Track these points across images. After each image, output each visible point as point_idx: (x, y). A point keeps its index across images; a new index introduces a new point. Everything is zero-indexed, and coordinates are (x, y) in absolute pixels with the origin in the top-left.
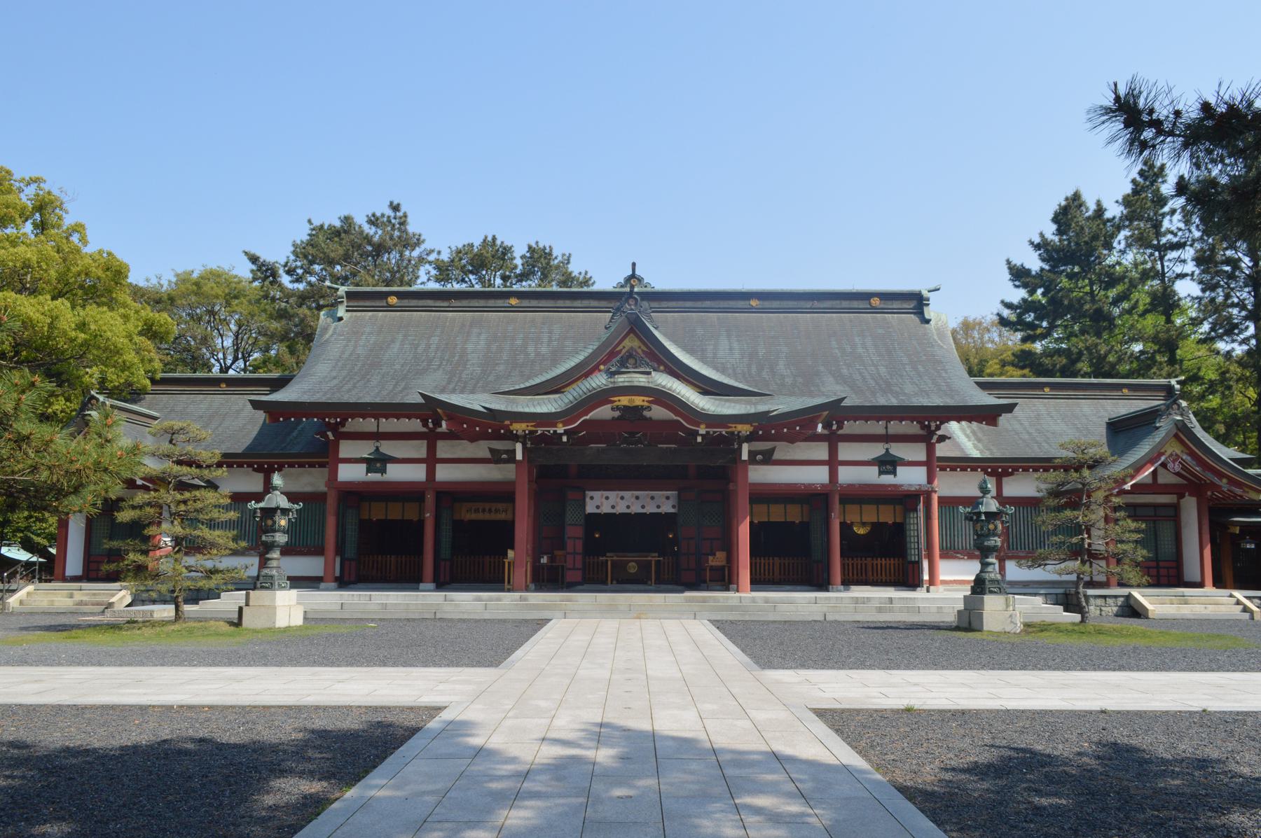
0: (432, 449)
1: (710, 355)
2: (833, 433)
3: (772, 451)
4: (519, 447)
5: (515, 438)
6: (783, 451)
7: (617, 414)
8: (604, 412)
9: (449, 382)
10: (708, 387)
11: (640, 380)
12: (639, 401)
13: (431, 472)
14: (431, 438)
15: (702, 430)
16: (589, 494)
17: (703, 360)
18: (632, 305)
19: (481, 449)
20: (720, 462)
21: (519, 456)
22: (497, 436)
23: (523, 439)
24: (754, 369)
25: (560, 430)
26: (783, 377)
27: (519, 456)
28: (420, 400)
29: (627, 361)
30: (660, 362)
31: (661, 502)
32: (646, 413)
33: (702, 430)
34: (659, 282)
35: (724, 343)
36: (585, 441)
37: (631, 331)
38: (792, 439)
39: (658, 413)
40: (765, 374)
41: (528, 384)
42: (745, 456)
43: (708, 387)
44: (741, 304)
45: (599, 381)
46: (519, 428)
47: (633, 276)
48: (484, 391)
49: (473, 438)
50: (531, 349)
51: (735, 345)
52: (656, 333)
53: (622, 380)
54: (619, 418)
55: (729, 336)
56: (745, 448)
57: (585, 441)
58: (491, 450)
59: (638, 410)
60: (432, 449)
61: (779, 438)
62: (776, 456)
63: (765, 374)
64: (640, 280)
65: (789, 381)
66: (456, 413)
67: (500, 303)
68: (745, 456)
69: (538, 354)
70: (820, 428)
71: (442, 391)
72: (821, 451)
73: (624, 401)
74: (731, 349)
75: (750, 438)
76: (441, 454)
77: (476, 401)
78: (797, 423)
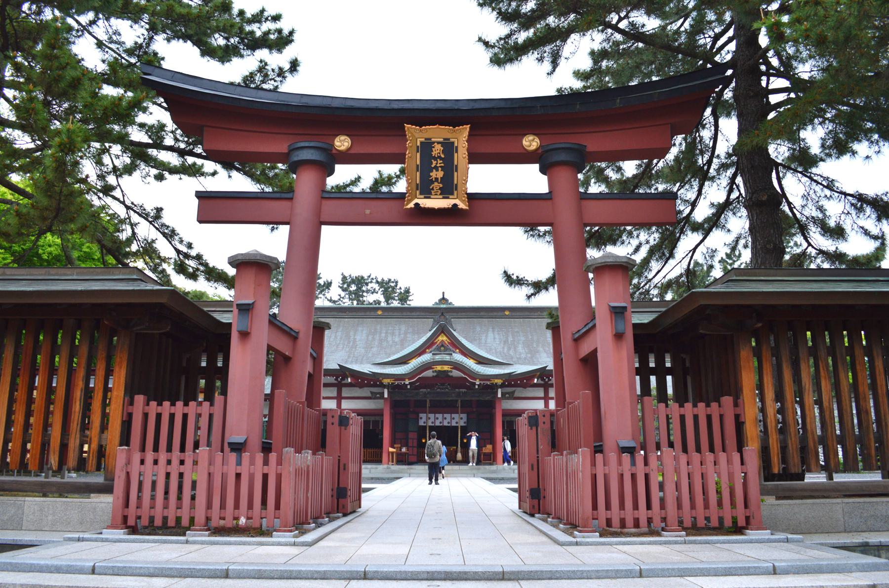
0: (339, 392)
1: (483, 341)
2: (546, 383)
3: (513, 392)
4: (386, 391)
5: (384, 386)
6: (519, 392)
7: (435, 374)
8: (429, 373)
9: (349, 357)
10: (481, 361)
11: (447, 358)
12: (446, 368)
13: (339, 405)
14: (339, 386)
15: (478, 382)
16: (421, 415)
17: (479, 346)
18: (443, 314)
19: (366, 392)
20: (487, 398)
21: (386, 396)
22: (375, 385)
23: (388, 386)
24: (506, 350)
25: (407, 382)
26: (520, 354)
27: (386, 396)
28: (338, 368)
29: (442, 348)
30: (457, 348)
31: (458, 420)
32: (450, 374)
33: (478, 382)
34: (458, 300)
35: (490, 334)
36: (417, 388)
37: (442, 332)
38: (525, 386)
39: (456, 373)
40: (511, 353)
41: (390, 359)
42: (499, 395)
43: (481, 361)
44: (500, 314)
45: (426, 357)
46: (386, 381)
47: (443, 298)
48: (368, 363)
49: (361, 386)
50: (390, 339)
51: (497, 336)
52: (455, 333)
53: (438, 358)
54: (436, 376)
55: (493, 331)
56: (500, 391)
57: (417, 388)
58: (372, 393)
59: (446, 372)
60: (339, 392)
61: (516, 385)
62: (516, 395)
63: (511, 353)
64: (447, 300)
65: (523, 356)
66: (355, 374)
67: (372, 313)
68: (499, 395)
69: (394, 342)
70: (536, 381)
71: (346, 362)
72: (540, 393)
73: (439, 368)
74: (494, 338)
75: (502, 386)
76: (344, 395)
77: (366, 368)
78: (524, 379)
